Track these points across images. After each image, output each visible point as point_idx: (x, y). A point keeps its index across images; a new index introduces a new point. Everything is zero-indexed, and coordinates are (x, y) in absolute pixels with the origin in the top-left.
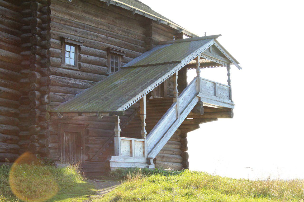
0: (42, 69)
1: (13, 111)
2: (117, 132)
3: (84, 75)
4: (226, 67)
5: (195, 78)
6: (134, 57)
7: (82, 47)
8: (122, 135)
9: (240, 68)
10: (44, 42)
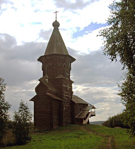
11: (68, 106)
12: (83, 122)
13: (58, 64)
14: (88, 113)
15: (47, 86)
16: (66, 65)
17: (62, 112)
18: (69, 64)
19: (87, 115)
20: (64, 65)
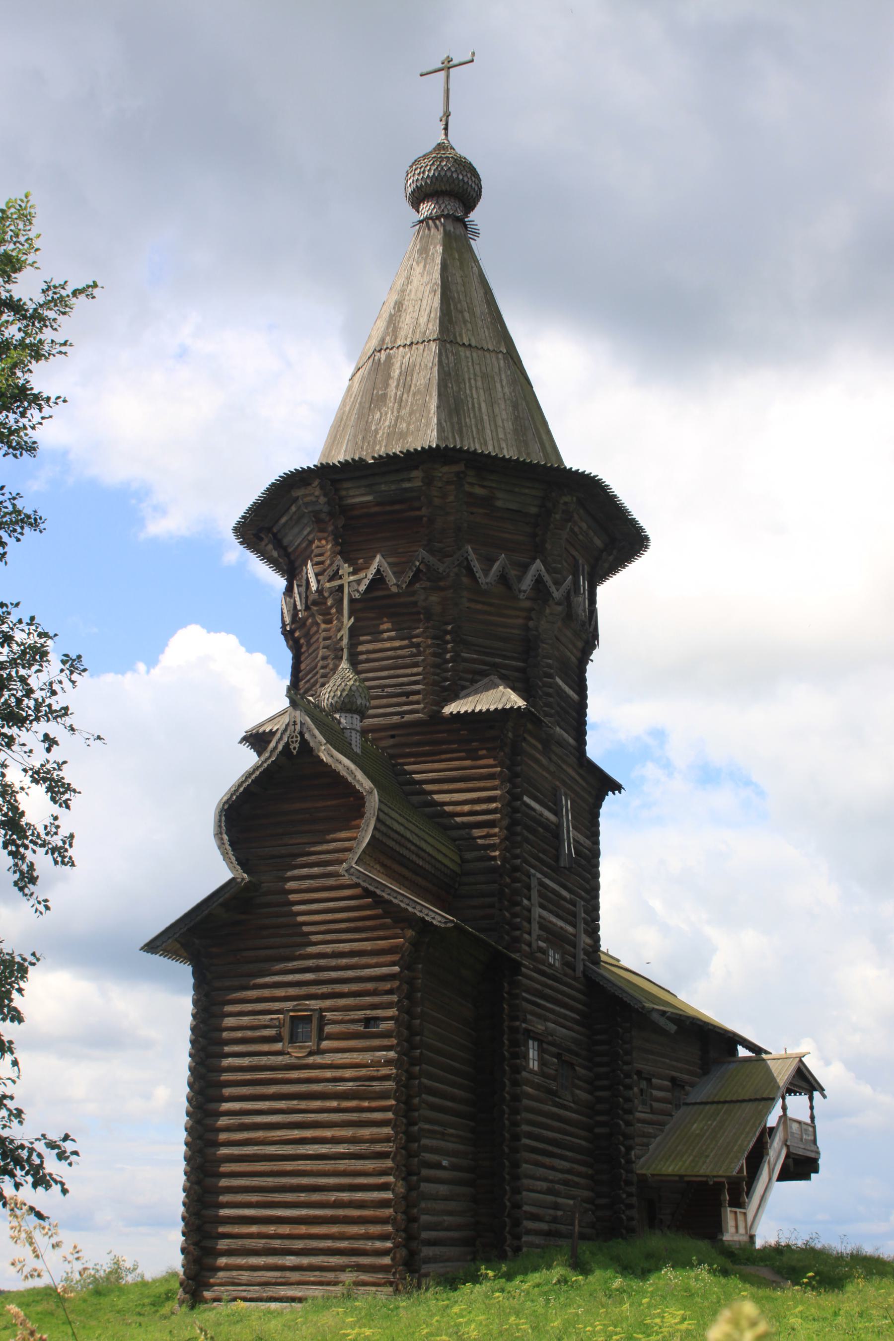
0: (627, 1117)
1: (590, 1172)
2: (725, 1200)
3: (655, 1117)
4: (807, 1097)
5: (780, 1117)
6: (692, 1085)
7: (654, 1081)
8: (730, 1206)
9: (824, 1097)
10: (628, 1081)
15: (362, 782)
16: (558, 583)
18: (584, 584)
20: (527, 583)
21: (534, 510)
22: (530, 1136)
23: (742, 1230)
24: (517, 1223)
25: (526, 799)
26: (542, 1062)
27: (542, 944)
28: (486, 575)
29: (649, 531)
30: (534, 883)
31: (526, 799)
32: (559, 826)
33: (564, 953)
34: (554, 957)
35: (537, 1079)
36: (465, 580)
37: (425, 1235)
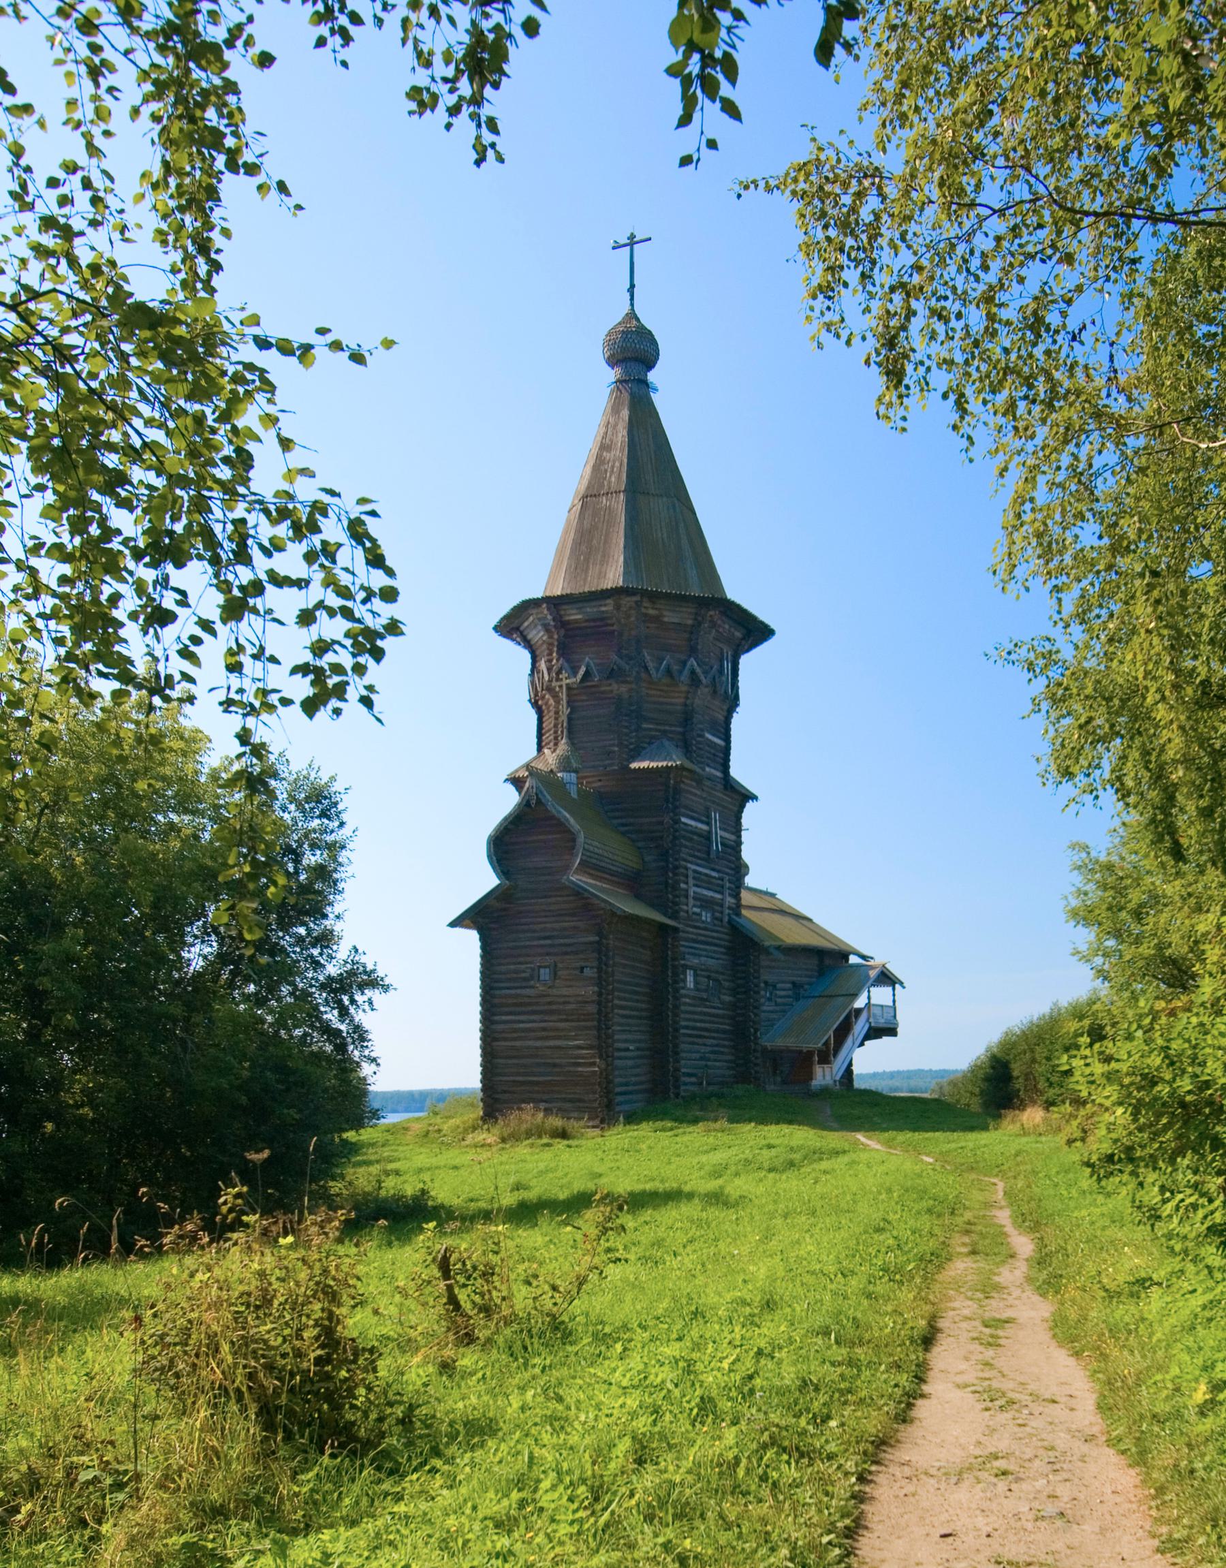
11: (711, 962)
12: (810, 1076)
13: (646, 668)
14: (848, 1017)
16: (705, 673)
17: (676, 1007)
18: (727, 666)
19: (844, 1031)
21: (690, 622)
22: (687, 1027)
23: (828, 1078)
24: (677, 1080)
25: (683, 820)
26: (696, 983)
27: (696, 910)
28: (657, 670)
29: (773, 626)
30: (690, 873)
31: (683, 820)
32: (710, 832)
33: (714, 911)
34: (706, 916)
35: (692, 994)
36: (643, 675)
37: (618, 1090)
